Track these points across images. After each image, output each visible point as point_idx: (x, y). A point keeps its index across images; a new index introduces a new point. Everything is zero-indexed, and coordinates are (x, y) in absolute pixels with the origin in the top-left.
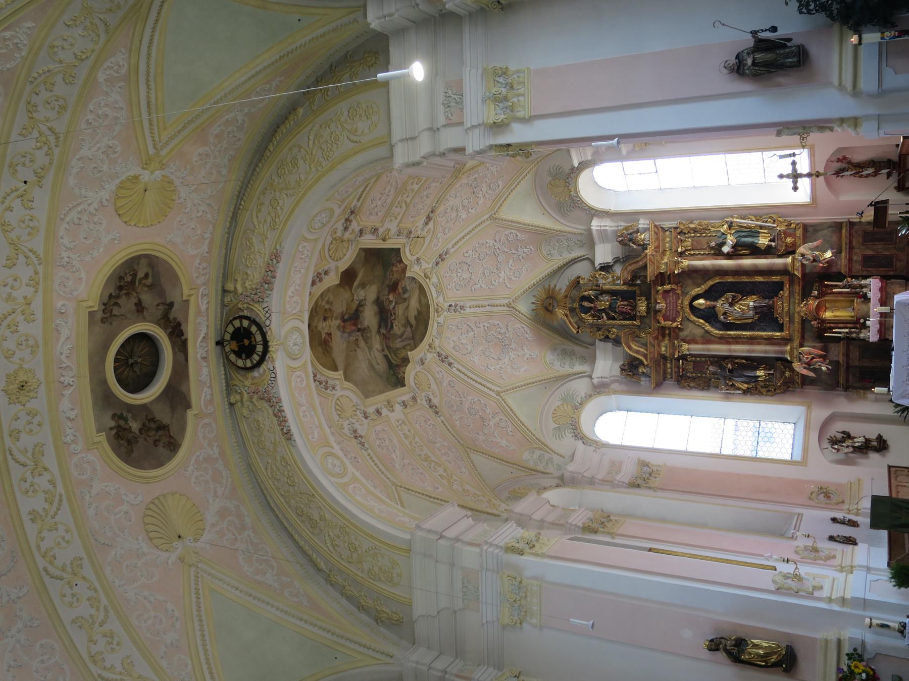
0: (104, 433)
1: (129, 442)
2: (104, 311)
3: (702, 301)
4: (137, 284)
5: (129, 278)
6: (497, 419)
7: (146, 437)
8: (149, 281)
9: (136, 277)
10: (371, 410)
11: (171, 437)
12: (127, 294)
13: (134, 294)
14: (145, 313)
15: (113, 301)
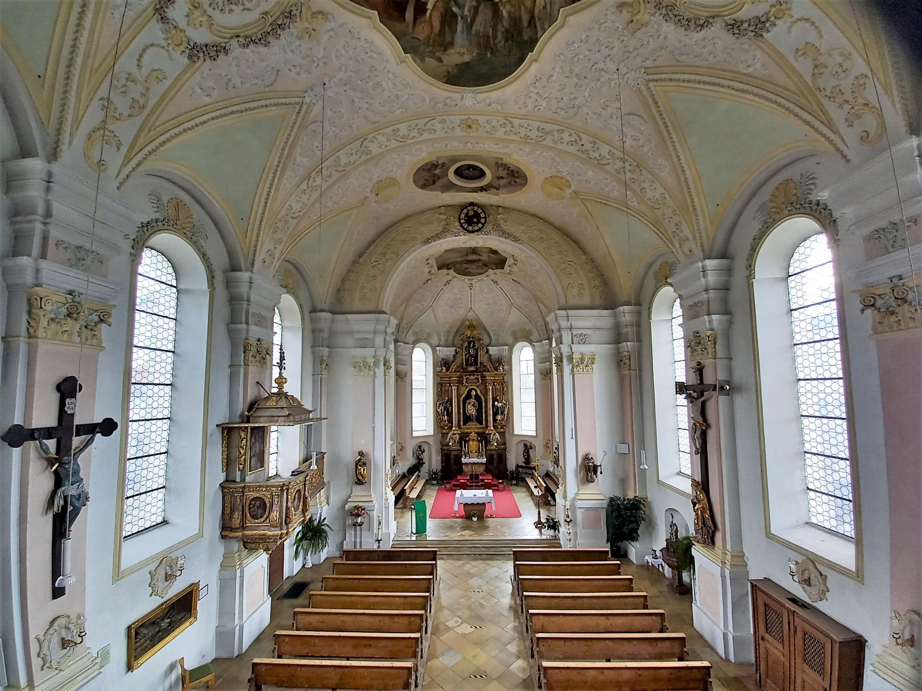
3: (475, 393)
5: (516, 175)
6: (420, 306)
10: (429, 261)
11: (429, 186)
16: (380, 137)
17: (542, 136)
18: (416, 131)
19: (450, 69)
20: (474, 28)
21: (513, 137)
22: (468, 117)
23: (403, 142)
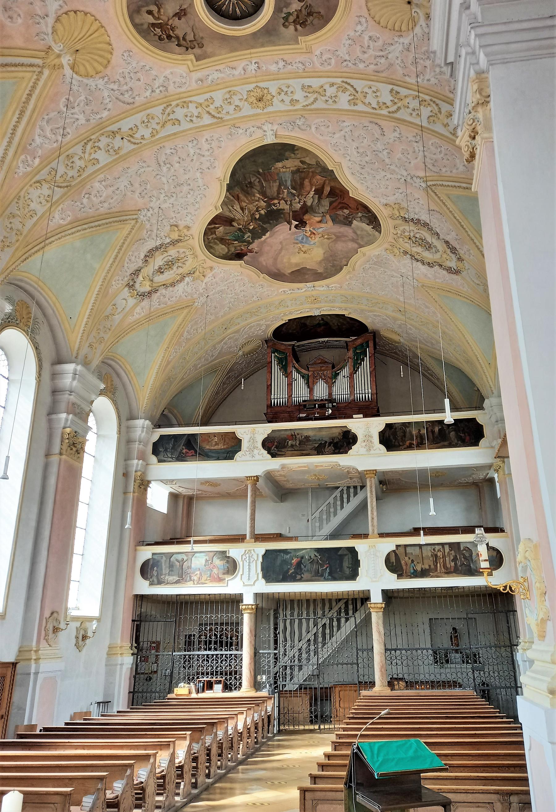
0: (299, 38)
1: (310, 14)
4: (161, 21)
5: (158, 30)
8: (154, 8)
9: (155, 24)
12: (173, 29)
14: (185, 7)
15: (182, 42)
16: (374, 105)
17: (169, 114)
18: (328, 94)
20: (278, 184)
22: (265, 111)
23: (346, 83)
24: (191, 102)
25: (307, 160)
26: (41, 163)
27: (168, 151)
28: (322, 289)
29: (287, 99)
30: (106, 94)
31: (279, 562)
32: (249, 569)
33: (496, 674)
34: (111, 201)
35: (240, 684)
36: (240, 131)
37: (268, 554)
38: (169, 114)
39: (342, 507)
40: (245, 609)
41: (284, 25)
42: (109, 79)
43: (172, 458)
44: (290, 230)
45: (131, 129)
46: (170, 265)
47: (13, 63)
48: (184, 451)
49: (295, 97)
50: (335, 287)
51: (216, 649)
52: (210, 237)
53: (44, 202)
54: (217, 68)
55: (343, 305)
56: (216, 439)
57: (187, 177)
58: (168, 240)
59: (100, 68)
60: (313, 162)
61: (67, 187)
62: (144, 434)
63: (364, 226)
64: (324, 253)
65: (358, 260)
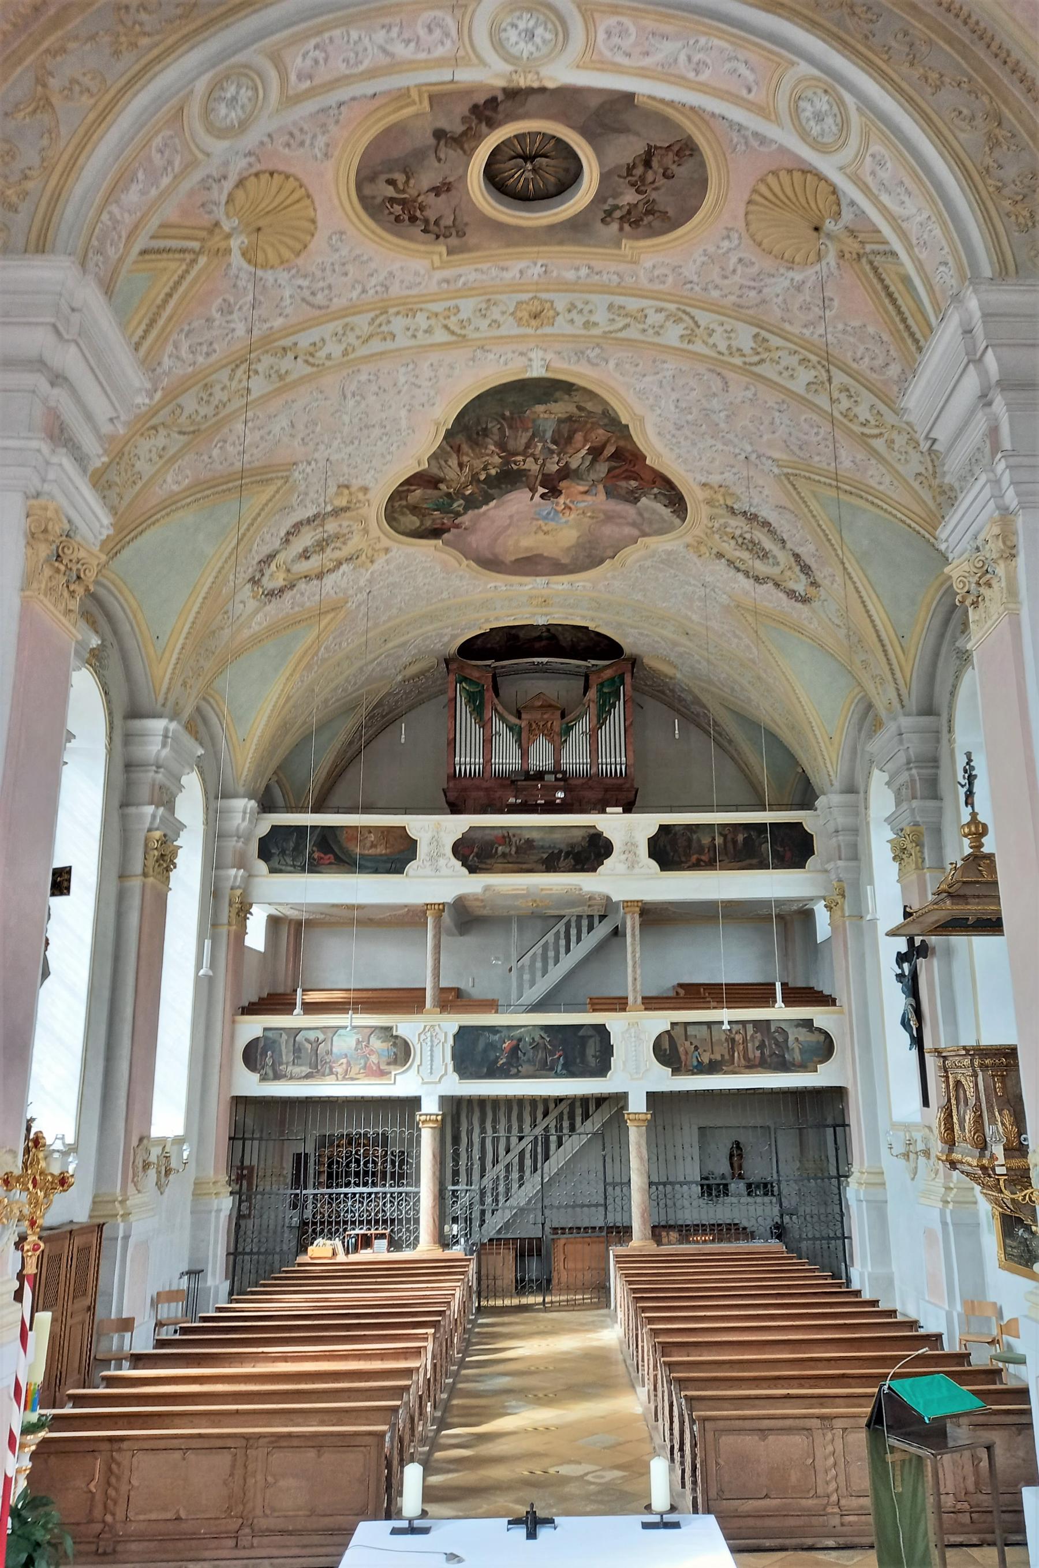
0: (624, 241)
1: (648, 212)
2: (446, 237)
5: (397, 209)
7: (653, 186)
12: (422, 208)
13: (420, 199)
15: (432, 227)
18: (649, 321)
19: (566, 397)
21: (437, 307)
22: (539, 332)
24: (421, 310)
25: (589, 406)
26: (164, 397)
27: (363, 377)
28: (560, 587)
29: (579, 320)
30: (287, 293)
31: (481, 1045)
32: (432, 1056)
33: (815, 1219)
34: (255, 451)
35: (417, 1239)
36: (491, 356)
37: (463, 1033)
38: (380, 325)
39: (568, 950)
40: (423, 1122)
41: (603, 220)
42: (298, 272)
43: (294, 866)
44: (532, 499)
45: (315, 344)
46: (321, 546)
47: (156, 247)
48: (316, 855)
49: (594, 318)
50: (584, 587)
51: (374, 1184)
52: (397, 504)
53: (155, 458)
54: (479, 266)
55: (590, 613)
56: (372, 837)
57: (384, 415)
58: (329, 508)
59: (287, 254)
60: (598, 409)
61: (194, 432)
62: (246, 823)
63: (659, 507)
64: (579, 537)
65: (632, 555)
